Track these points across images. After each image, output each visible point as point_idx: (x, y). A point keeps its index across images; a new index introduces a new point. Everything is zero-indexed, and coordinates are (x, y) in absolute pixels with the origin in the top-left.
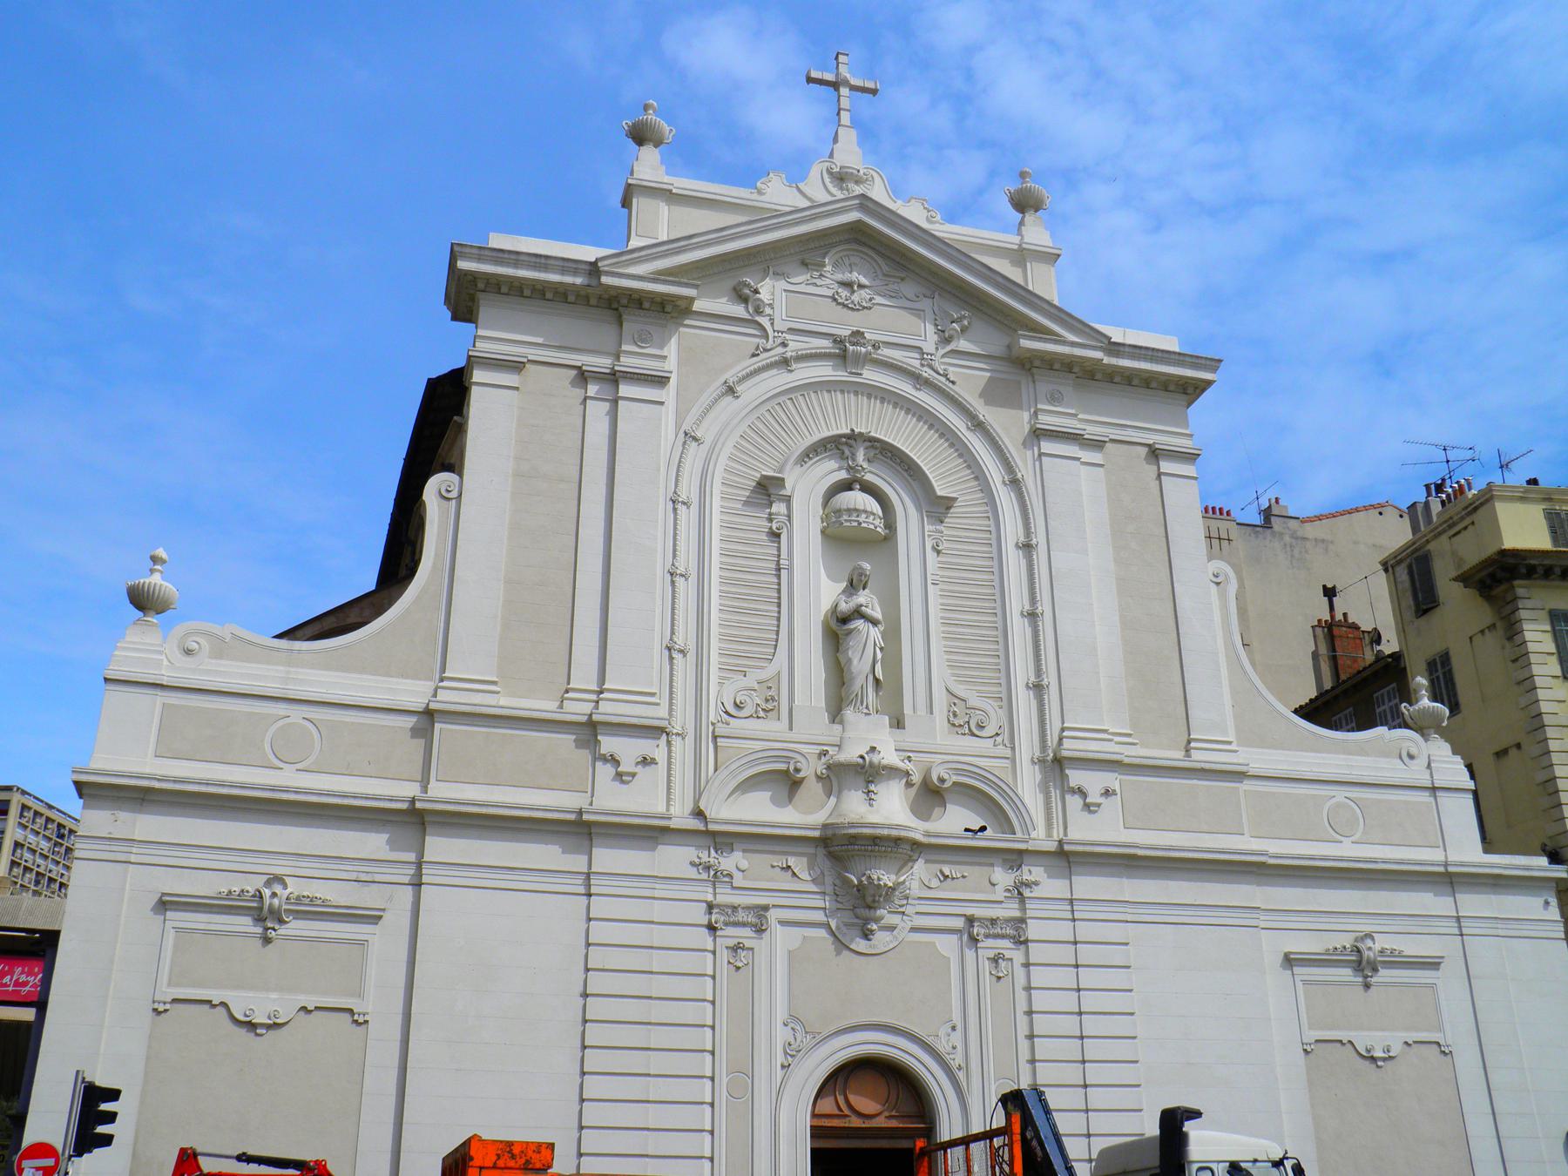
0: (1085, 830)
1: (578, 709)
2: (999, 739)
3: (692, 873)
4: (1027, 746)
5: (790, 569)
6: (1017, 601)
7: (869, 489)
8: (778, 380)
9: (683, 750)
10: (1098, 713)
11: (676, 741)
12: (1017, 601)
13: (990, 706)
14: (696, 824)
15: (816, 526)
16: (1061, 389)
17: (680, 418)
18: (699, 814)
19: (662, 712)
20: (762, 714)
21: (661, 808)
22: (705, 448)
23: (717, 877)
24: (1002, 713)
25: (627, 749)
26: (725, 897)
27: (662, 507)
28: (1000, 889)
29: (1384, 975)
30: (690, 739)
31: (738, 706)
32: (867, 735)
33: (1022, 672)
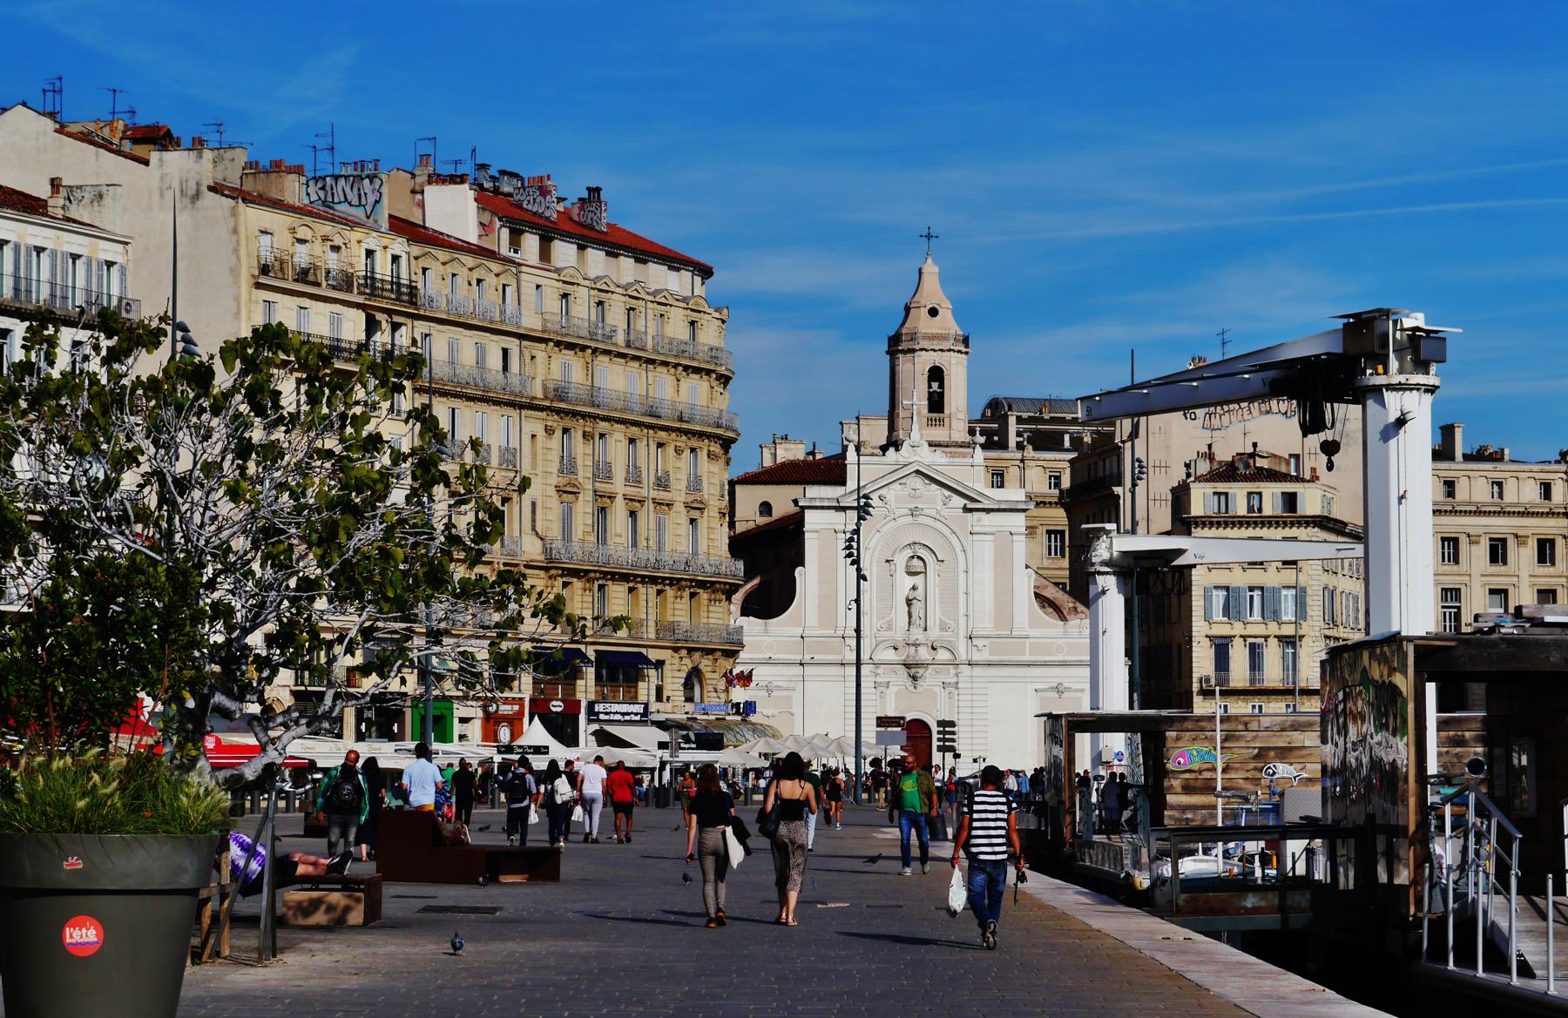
0: (976, 657)
1: (840, 633)
4: (962, 633)
6: (962, 589)
7: (919, 558)
10: (985, 623)
12: (962, 589)
29: (1066, 695)
32: (917, 634)
33: (962, 610)
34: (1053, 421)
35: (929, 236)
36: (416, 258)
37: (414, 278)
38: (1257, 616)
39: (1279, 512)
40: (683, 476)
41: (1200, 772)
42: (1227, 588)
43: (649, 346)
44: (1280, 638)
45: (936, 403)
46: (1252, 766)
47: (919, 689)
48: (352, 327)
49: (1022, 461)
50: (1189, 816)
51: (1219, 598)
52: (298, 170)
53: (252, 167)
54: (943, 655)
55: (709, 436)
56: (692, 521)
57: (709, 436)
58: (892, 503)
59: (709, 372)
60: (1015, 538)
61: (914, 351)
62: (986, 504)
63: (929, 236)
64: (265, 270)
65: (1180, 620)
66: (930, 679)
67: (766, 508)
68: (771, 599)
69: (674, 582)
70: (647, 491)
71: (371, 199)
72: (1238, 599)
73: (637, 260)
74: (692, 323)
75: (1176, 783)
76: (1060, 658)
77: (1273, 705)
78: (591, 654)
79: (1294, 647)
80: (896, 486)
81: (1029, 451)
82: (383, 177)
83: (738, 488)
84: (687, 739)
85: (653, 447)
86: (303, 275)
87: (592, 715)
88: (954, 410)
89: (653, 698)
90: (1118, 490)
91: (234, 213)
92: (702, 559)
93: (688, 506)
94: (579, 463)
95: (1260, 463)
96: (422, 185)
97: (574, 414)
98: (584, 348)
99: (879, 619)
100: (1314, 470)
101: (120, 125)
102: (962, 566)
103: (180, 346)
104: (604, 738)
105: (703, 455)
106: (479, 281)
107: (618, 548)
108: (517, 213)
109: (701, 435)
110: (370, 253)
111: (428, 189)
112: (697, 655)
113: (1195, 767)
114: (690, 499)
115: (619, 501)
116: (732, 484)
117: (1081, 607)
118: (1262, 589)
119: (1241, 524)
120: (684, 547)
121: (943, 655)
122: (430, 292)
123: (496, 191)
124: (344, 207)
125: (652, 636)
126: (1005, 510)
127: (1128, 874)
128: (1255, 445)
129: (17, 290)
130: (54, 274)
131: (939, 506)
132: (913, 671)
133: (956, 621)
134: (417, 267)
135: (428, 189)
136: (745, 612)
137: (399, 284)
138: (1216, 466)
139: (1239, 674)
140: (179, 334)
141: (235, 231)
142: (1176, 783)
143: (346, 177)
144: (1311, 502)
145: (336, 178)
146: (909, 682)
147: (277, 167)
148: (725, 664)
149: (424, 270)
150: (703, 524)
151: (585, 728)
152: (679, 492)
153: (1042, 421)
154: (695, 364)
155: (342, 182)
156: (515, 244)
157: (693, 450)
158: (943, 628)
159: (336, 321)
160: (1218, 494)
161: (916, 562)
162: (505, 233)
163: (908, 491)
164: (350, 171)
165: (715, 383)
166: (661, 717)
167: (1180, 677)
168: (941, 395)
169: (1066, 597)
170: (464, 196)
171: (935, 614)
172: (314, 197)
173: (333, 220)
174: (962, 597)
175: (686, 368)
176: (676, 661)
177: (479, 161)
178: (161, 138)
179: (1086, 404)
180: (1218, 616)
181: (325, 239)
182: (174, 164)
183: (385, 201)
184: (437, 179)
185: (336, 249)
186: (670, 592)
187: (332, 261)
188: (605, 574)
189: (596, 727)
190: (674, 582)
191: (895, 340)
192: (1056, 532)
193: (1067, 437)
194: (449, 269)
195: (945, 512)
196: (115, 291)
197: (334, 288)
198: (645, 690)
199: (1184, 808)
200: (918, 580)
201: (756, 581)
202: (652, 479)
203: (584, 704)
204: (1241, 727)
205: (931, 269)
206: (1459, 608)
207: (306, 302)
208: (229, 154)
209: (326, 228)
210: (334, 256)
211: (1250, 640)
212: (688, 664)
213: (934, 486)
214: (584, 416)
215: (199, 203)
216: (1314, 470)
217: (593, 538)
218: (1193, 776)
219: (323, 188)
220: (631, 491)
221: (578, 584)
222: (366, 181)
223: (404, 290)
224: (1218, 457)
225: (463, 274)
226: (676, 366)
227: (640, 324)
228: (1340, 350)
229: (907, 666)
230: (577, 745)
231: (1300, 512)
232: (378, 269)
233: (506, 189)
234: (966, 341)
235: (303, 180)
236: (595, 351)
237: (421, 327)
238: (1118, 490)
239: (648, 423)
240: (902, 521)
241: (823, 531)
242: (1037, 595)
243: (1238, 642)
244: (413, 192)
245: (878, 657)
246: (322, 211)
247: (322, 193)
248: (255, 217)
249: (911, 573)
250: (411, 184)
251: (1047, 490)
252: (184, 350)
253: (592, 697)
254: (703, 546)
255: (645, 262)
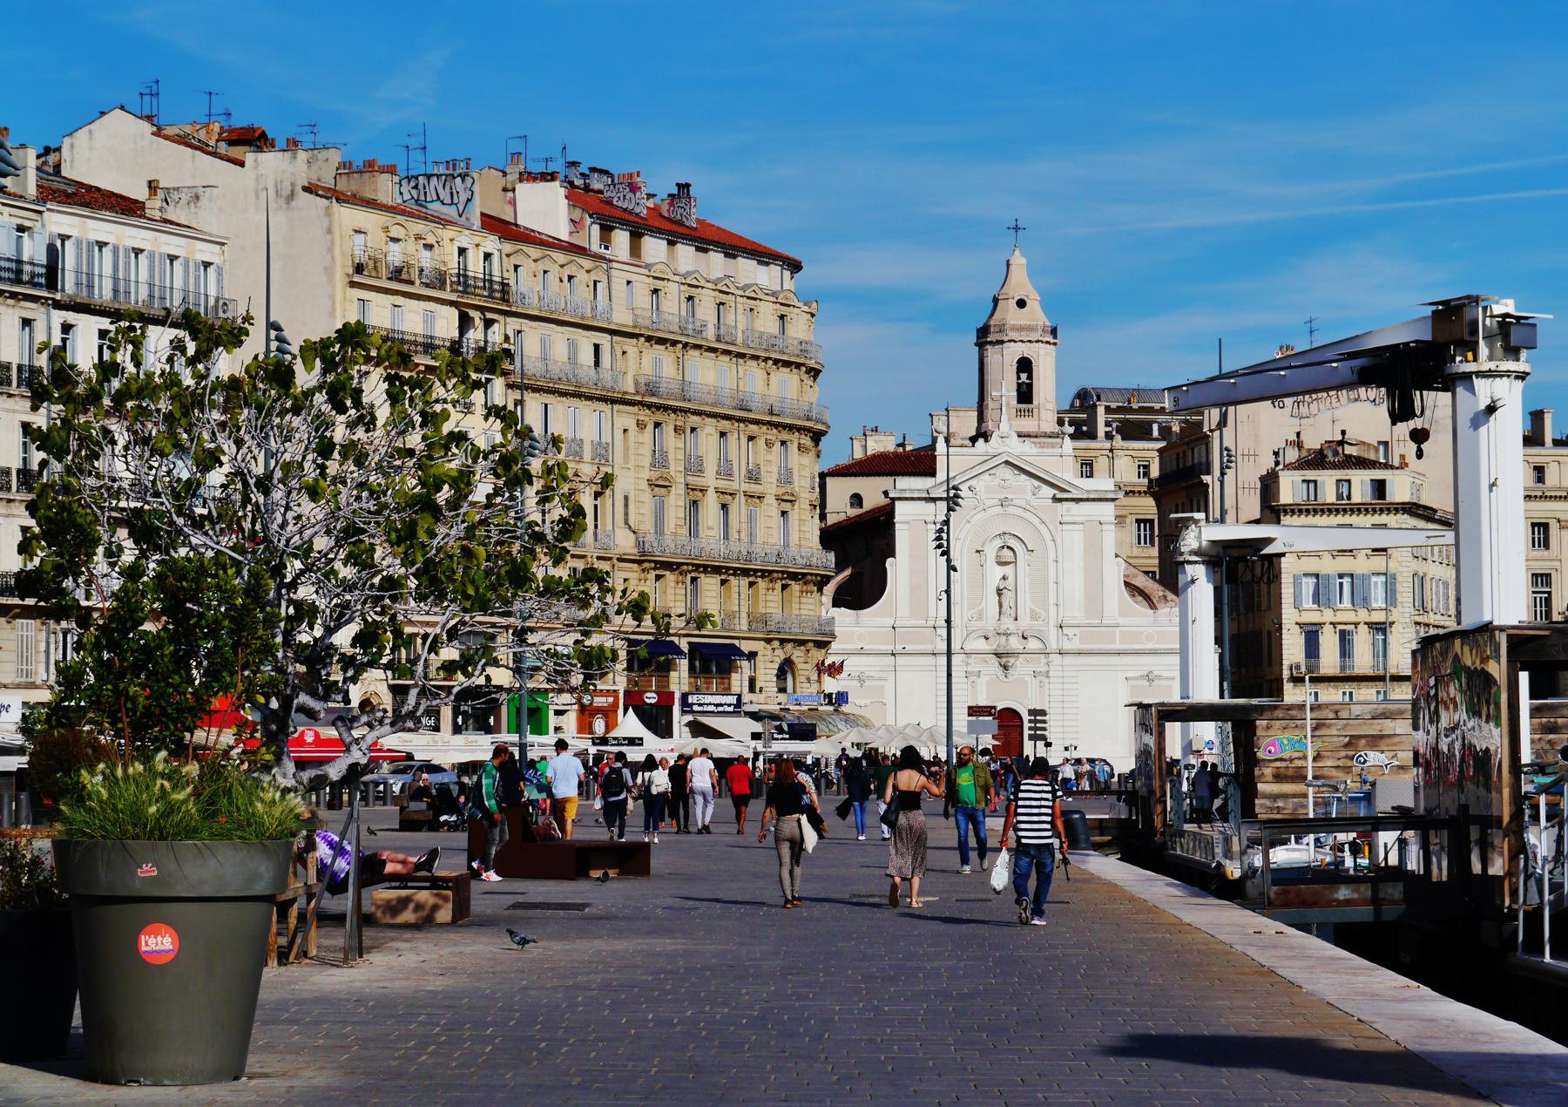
0: (1067, 646)
1: (931, 623)
4: (1053, 622)
6: (1052, 578)
10: (1074, 612)
12: (1052, 578)
26: (970, 669)
32: (1008, 624)
33: (1052, 600)
34: (1142, 410)
35: (1017, 228)
36: (508, 255)
37: (506, 275)
38: (1347, 603)
39: (1368, 499)
40: (775, 469)
41: (1291, 760)
42: (1317, 576)
43: (739, 340)
44: (1370, 625)
45: (1025, 394)
46: (1343, 754)
47: (1011, 678)
48: (445, 325)
49: (1111, 450)
50: (1280, 804)
51: (1308, 585)
52: (392, 170)
53: (346, 168)
54: (1033, 645)
55: (799, 429)
56: (784, 513)
57: (799, 429)
58: (982, 494)
59: (798, 366)
61: (1002, 342)
62: (1076, 494)
63: (1017, 228)
64: (359, 269)
65: (1269, 608)
66: (1021, 667)
67: (857, 499)
68: (862, 590)
69: (765, 574)
70: (739, 484)
71: (464, 197)
72: (1327, 586)
73: (727, 255)
74: (782, 317)
75: (1268, 771)
76: (1150, 646)
77: (1363, 691)
78: (685, 648)
79: (1385, 634)
80: (986, 476)
81: (1118, 441)
82: (476, 176)
83: (829, 480)
84: (780, 730)
85: (744, 440)
86: (397, 274)
87: (686, 706)
88: (1042, 400)
89: (746, 689)
90: (1206, 479)
91: (328, 212)
92: (793, 551)
93: (779, 499)
94: (671, 456)
95: (1349, 450)
96: (513, 183)
97: (666, 408)
98: (674, 343)
100: (1402, 457)
101: (216, 128)
102: (1052, 556)
103: (274, 345)
104: (698, 729)
105: (793, 448)
106: (570, 278)
107: (711, 541)
108: (607, 210)
109: (791, 428)
110: (462, 251)
111: (519, 187)
112: (790, 646)
113: (1286, 755)
114: (781, 491)
115: (711, 494)
116: (823, 476)
117: (1170, 596)
118: (1352, 576)
119: (1330, 511)
120: (776, 539)
121: (1033, 645)
122: (522, 289)
123: (587, 188)
124: (436, 206)
125: (745, 627)
126: (1094, 500)
127: (1219, 864)
128: (1343, 432)
129: (116, 291)
130: (152, 275)
131: (1029, 496)
132: (1003, 661)
133: (1047, 610)
134: (509, 264)
135: (519, 187)
136: (837, 603)
137: (491, 281)
138: (1304, 454)
139: (1329, 661)
140: (273, 334)
141: (329, 231)
142: (1268, 771)
143: (438, 176)
144: (1400, 490)
145: (429, 177)
146: (1000, 671)
147: (370, 167)
148: (817, 655)
149: (516, 267)
150: (794, 516)
151: (679, 720)
152: (770, 486)
153: (1130, 410)
154: (785, 358)
155: (434, 180)
156: (606, 240)
157: (783, 443)
158: (1034, 617)
159: (429, 318)
160: (1308, 482)
161: (1006, 552)
162: (596, 229)
163: (997, 481)
164: (442, 170)
165: (805, 377)
166: (754, 708)
167: (1270, 664)
168: (1030, 386)
169: (1156, 585)
170: (555, 193)
172: (407, 196)
173: (425, 219)
174: (1052, 587)
175: (776, 362)
176: (769, 652)
177: (570, 159)
178: (254, 139)
179: (1173, 394)
180: (1308, 603)
181: (418, 237)
182: (268, 165)
183: (477, 198)
184: (528, 176)
185: (429, 247)
186: (762, 584)
187: (426, 259)
188: (697, 566)
189: (689, 718)
190: (765, 574)
191: (983, 332)
192: (1145, 521)
193: (1155, 427)
194: (541, 266)
195: (1035, 502)
196: (212, 292)
197: (427, 285)
198: (738, 681)
199: (1275, 797)
200: (1009, 570)
201: (848, 572)
202: (743, 472)
203: (677, 696)
204: (1331, 715)
205: (1019, 261)
206: (1549, 593)
207: (400, 300)
208: (323, 155)
209: (419, 227)
210: (427, 254)
211: (1340, 627)
212: (780, 655)
213: (1023, 477)
214: (675, 410)
215: (294, 204)
216: (1402, 457)
217: (685, 531)
218: (1284, 764)
219: (416, 187)
220: (723, 484)
221: (670, 577)
222: (458, 180)
223: (496, 287)
224: (1306, 446)
225: (554, 271)
226: (766, 359)
227: (729, 318)
228: (1429, 337)
229: (998, 655)
230: (671, 736)
231: (1389, 499)
232: (470, 267)
233: (596, 186)
234: (1054, 332)
235: (396, 179)
236: (685, 345)
237: (514, 324)
238: (1206, 479)
239: (739, 417)
241: (913, 523)
242: (1127, 584)
243: (1328, 629)
244: (505, 190)
245: (968, 648)
246: (416, 210)
247: (414, 193)
248: (349, 216)
249: (1001, 564)
250: (502, 182)
251: (1135, 479)
252: (278, 350)
253: (686, 689)
254: (794, 538)
255: (734, 257)
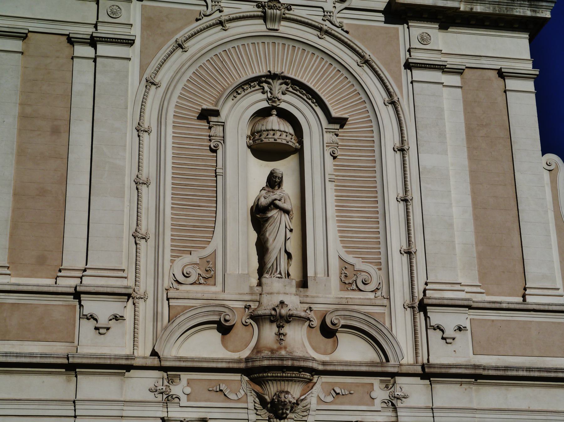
1: (68, 283)
2: (379, 293)
3: (151, 397)
4: (400, 295)
5: (224, 176)
8: (215, 35)
9: (145, 309)
10: (454, 269)
11: (141, 304)
12: (394, 189)
13: (371, 269)
14: (155, 362)
15: (243, 142)
16: (429, 31)
17: (143, 69)
18: (154, 353)
19: (130, 282)
20: (202, 281)
21: (128, 351)
22: (161, 90)
23: (169, 399)
24: (382, 273)
25: (102, 309)
27: (131, 135)
28: (377, 402)
30: (150, 301)
31: (186, 276)
54: (352, 351)
60: (511, 84)
99: (177, 252)
102: (390, 138)
121: (352, 351)
132: (272, 390)
133: (384, 266)
158: (350, 280)
161: (274, 122)
171: (327, 245)
174: (395, 211)
229: (255, 373)
240: (237, 29)
249: (263, 150)
